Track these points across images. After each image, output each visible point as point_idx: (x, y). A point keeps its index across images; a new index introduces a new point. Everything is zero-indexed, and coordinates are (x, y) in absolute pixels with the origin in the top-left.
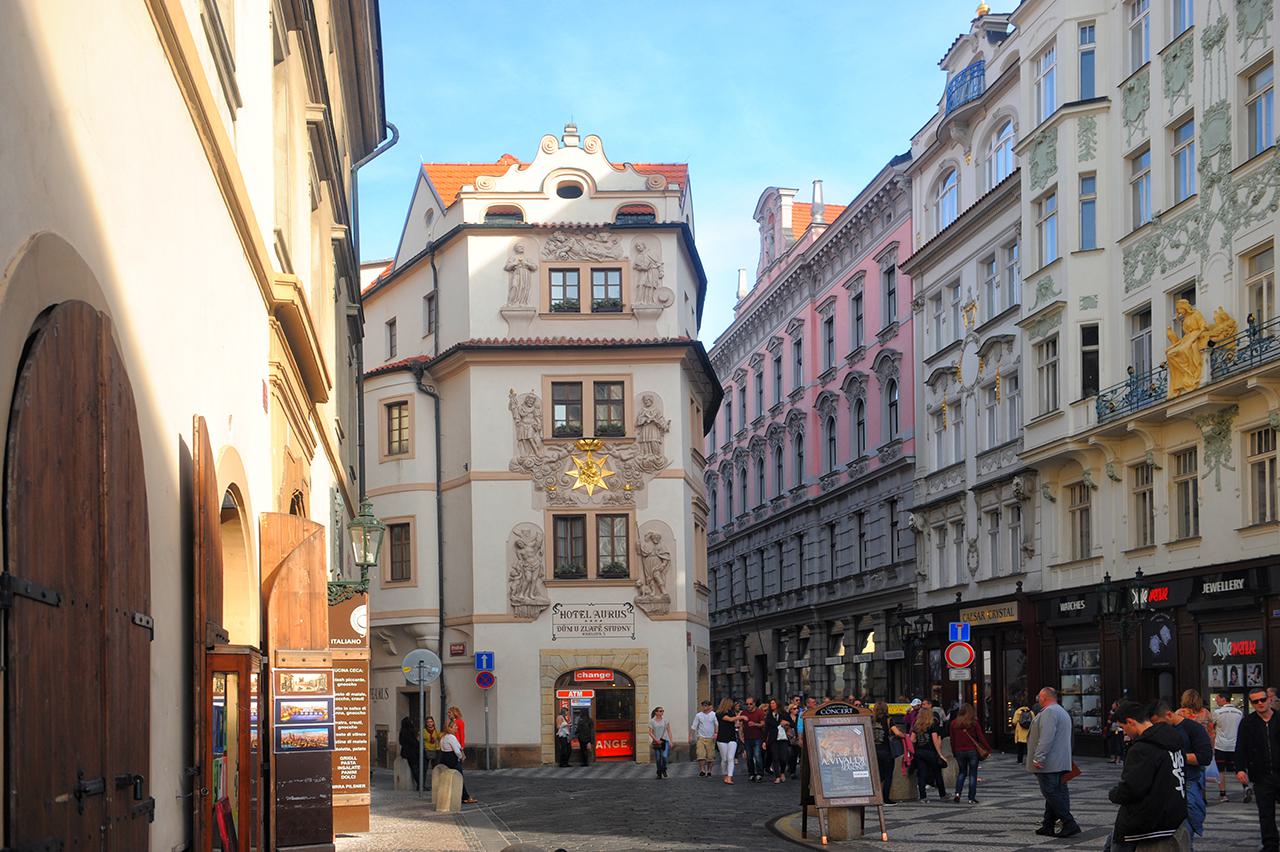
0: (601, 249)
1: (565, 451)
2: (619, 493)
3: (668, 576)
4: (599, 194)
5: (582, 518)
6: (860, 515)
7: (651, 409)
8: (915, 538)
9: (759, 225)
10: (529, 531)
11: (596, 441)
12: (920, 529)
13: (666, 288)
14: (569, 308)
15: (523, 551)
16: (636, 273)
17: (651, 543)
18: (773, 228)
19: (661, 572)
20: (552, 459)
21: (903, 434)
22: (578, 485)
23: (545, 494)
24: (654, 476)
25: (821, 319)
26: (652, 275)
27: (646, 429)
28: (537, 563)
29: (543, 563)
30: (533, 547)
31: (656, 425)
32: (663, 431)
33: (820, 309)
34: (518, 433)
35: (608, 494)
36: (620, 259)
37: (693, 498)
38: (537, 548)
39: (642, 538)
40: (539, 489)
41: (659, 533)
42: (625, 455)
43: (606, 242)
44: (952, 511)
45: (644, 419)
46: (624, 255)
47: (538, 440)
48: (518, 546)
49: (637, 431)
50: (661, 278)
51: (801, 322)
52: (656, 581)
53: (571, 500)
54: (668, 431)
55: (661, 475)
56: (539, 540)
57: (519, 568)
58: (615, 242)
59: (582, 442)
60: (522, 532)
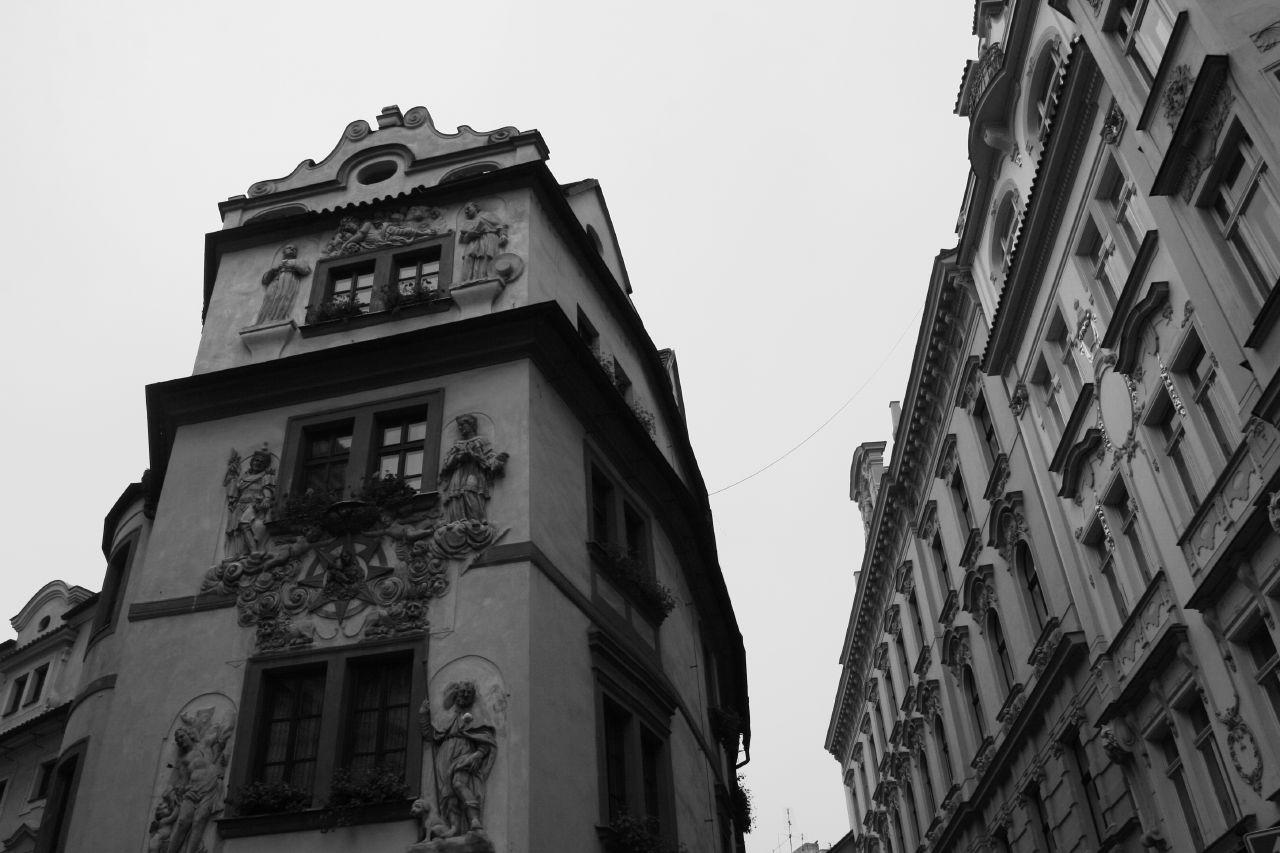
0: (411, 227)
2: (397, 608)
4: (418, 166)
6: (1032, 794)
8: (1125, 780)
9: (857, 504)
10: (211, 711)
12: (1126, 748)
14: (351, 316)
18: (869, 496)
21: (1057, 606)
23: (255, 629)
25: (926, 545)
26: (488, 243)
30: (212, 744)
32: (496, 475)
33: (922, 534)
37: (591, 636)
42: (411, 531)
44: (1174, 686)
47: (259, 523)
48: (183, 748)
50: (503, 245)
51: (909, 565)
52: (456, 794)
53: (302, 636)
57: (173, 797)
58: (435, 216)
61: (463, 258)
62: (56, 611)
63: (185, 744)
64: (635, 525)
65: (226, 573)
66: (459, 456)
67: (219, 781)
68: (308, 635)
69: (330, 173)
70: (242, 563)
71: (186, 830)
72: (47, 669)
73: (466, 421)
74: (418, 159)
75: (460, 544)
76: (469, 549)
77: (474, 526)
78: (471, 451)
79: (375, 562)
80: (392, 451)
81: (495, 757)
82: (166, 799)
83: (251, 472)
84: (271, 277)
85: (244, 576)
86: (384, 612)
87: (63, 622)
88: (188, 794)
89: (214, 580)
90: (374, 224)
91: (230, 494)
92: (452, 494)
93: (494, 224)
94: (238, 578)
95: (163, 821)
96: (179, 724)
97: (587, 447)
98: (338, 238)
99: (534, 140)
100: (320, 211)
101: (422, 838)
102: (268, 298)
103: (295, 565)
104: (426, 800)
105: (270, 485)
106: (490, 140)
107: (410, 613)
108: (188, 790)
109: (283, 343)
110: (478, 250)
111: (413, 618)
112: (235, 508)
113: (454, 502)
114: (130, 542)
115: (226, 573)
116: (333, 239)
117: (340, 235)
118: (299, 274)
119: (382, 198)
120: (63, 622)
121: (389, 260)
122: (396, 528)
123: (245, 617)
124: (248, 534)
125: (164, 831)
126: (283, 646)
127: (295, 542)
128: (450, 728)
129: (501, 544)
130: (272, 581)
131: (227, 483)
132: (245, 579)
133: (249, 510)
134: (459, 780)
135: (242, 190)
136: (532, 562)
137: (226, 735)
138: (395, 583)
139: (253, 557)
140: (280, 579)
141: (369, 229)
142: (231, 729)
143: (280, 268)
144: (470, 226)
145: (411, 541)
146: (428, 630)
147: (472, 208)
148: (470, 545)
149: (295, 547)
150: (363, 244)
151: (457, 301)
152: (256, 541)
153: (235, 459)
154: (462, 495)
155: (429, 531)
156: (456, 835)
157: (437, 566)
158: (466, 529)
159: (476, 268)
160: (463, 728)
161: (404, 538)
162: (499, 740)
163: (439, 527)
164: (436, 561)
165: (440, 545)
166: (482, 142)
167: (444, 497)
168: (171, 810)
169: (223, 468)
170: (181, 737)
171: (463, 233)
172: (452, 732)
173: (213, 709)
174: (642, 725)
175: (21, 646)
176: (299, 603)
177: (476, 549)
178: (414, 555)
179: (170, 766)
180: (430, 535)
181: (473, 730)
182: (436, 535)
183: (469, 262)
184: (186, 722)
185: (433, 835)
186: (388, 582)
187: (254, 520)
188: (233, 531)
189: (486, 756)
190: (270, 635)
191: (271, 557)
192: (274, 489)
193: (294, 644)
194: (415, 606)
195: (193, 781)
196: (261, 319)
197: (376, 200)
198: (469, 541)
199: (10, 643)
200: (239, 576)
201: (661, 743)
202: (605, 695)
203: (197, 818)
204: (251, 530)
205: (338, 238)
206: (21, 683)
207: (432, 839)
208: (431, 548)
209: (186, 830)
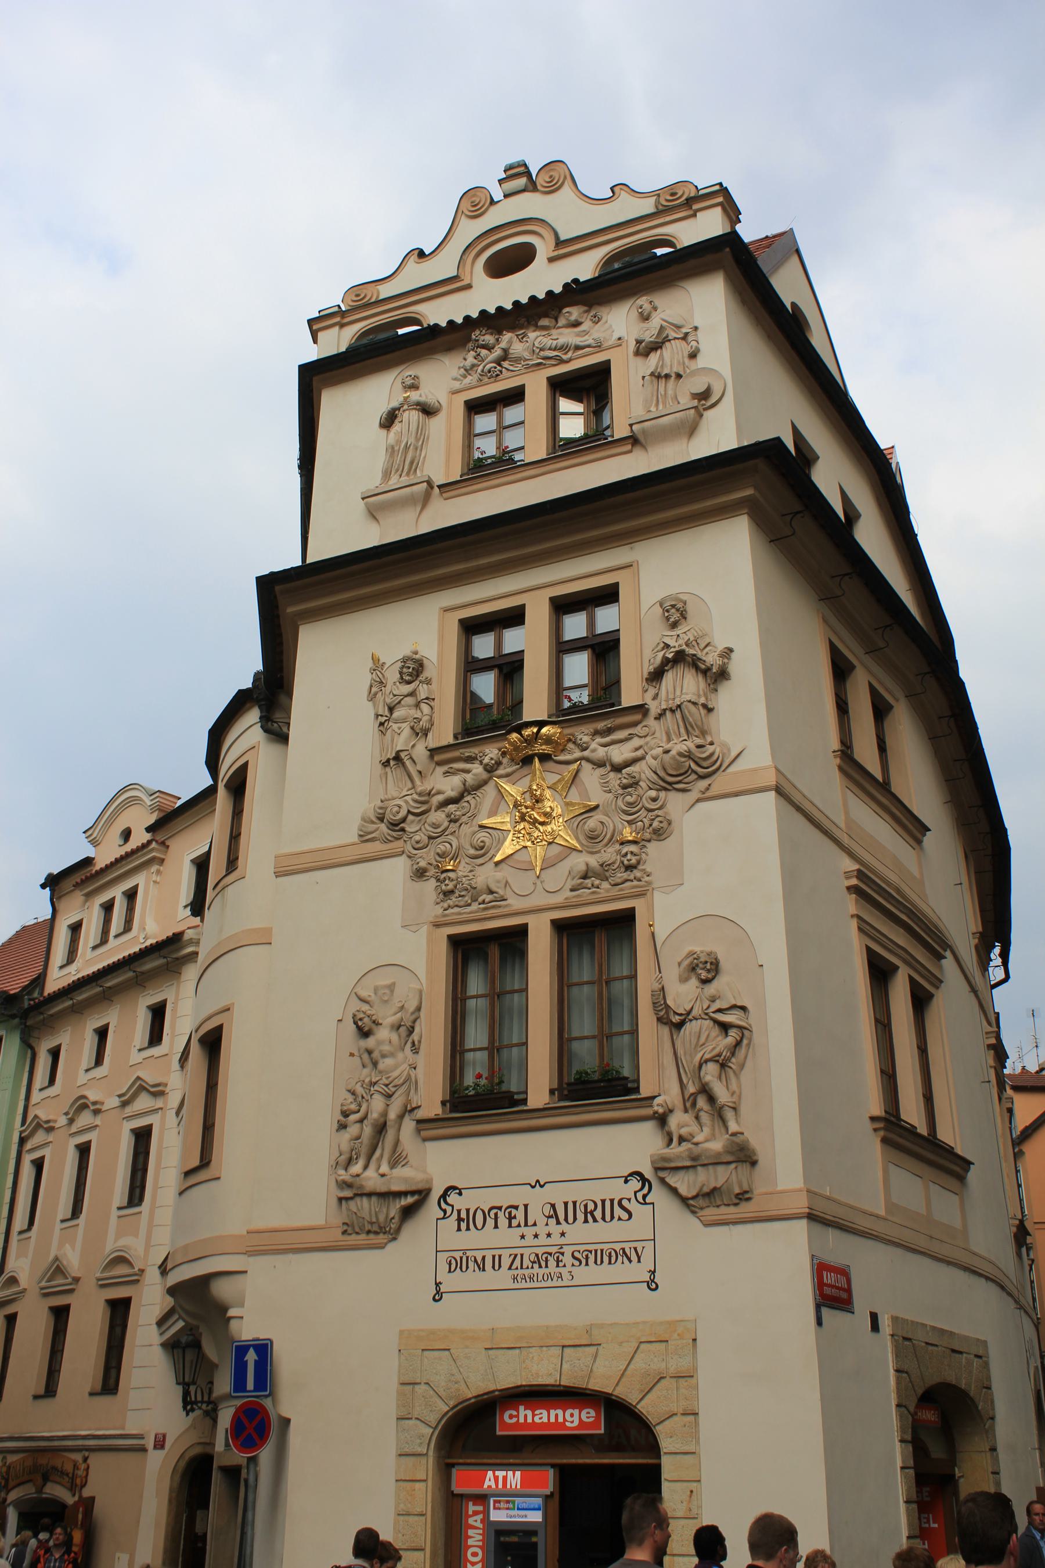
0: (567, 336)
1: (477, 769)
2: (610, 854)
3: (746, 1076)
5: (521, 932)
7: (679, 631)
10: (391, 987)
11: (544, 730)
13: (704, 368)
15: (370, 1042)
16: (640, 360)
17: (694, 982)
19: (723, 1066)
20: (451, 793)
22: (508, 848)
23: (432, 883)
24: (694, 795)
26: (671, 356)
27: (669, 678)
28: (399, 1072)
29: (420, 1073)
30: (397, 1027)
31: (695, 663)
34: (382, 749)
35: (579, 862)
36: (605, 345)
38: (407, 1029)
39: (671, 974)
40: (420, 874)
41: (708, 949)
42: (619, 754)
43: (576, 324)
45: (661, 655)
46: (616, 336)
47: (420, 751)
49: (652, 691)
50: (693, 356)
52: (705, 1090)
53: (491, 892)
54: (723, 675)
55: (714, 791)
56: (412, 1006)
57: (360, 1090)
58: (596, 320)
59: (514, 736)
60: (376, 990)
61: (644, 377)
62: (140, 820)
63: (366, 1029)
64: (881, 711)
65: (389, 816)
66: (670, 656)
67: (413, 1073)
68: (501, 892)
69: (443, 267)
70: (406, 802)
71: (381, 1129)
72: (136, 893)
73: (673, 606)
74: (562, 238)
75: (682, 771)
76: (694, 777)
77: (699, 747)
78: (684, 647)
79: (574, 796)
80: (576, 646)
81: (749, 1045)
82: (353, 1093)
83: (402, 681)
84: (389, 420)
85: (411, 817)
86: (593, 861)
87: (148, 836)
88: (376, 1088)
89: (373, 822)
90: (517, 335)
91: (380, 713)
92: (664, 707)
93: (678, 327)
94: (404, 820)
95: (353, 1117)
96: (356, 1005)
97: (825, 621)
98: (471, 359)
99: (721, 199)
100: (444, 324)
101: (670, 1141)
102: (391, 450)
103: (473, 802)
104: (670, 1095)
105: (427, 698)
106: (657, 203)
107: (626, 862)
108: (375, 1083)
109: (419, 509)
110: (662, 366)
111: (629, 868)
112: (387, 729)
113: (668, 713)
114: (245, 766)
115: (389, 816)
116: (465, 359)
117: (472, 353)
118: (428, 411)
119: (524, 300)
120: (148, 836)
121: (544, 385)
122: (597, 749)
123: (418, 870)
124: (408, 763)
125: (353, 1130)
126: (469, 905)
127: (468, 771)
128: (692, 1008)
129: (730, 770)
130: (446, 824)
131: (372, 697)
132: (413, 822)
133: (407, 732)
134: (710, 1072)
135: (333, 298)
136: (779, 791)
137: (414, 1017)
138: (602, 823)
139: (420, 794)
140: (455, 821)
141: (510, 342)
142: (419, 1009)
143: (402, 405)
144: (649, 332)
145: (617, 768)
146: (649, 883)
147: (647, 307)
148: (696, 773)
149: (469, 777)
150: (505, 364)
151: (641, 438)
152: (420, 772)
153: (377, 666)
154: (679, 706)
155: (639, 753)
156: (707, 1141)
157: (654, 800)
158: (689, 751)
159: (662, 390)
160: (708, 1007)
161: (607, 765)
162: (753, 1020)
163: (652, 749)
164: (653, 793)
165: (655, 773)
166: (647, 206)
167: (654, 708)
168: (360, 1106)
169: (367, 679)
170: (361, 1019)
171: (639, 342)
172: (694, 1013)
173: (394, 984)
174: (911, 978)
175: (100, 864)
176: (481, 852)
177: (702, 777)
178: (625, 787)
179: (352, 1055)
180: (642, 758)
181: (719, 1011)
182: (648, 757)
183: (652, 382)
184: (363, 1000)
185: (682, 1139)
186: (592, 823)
187: (413, 746)
188: (388, 761)
189: (738, 1043)
190: (452, 892)
191: (439, 793)
192: (432, 703)
193: (484, 901)
194: (632, 853)
195: (380, 1072)
196: (387, 475)
197: (516, 304)
198: (693, 766)
199: (87, 862)
200: (404, 820)
201: (930, 996)
202: (868, 949)
203: (392, 1115)
204: (411, 758)
205: (471, 359)
206: (108, 907)
207: (680, 1144)
208: (643, 776)
209: (381, 1129)
